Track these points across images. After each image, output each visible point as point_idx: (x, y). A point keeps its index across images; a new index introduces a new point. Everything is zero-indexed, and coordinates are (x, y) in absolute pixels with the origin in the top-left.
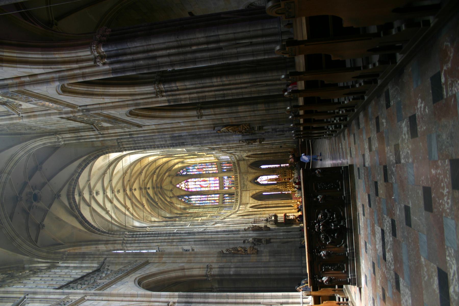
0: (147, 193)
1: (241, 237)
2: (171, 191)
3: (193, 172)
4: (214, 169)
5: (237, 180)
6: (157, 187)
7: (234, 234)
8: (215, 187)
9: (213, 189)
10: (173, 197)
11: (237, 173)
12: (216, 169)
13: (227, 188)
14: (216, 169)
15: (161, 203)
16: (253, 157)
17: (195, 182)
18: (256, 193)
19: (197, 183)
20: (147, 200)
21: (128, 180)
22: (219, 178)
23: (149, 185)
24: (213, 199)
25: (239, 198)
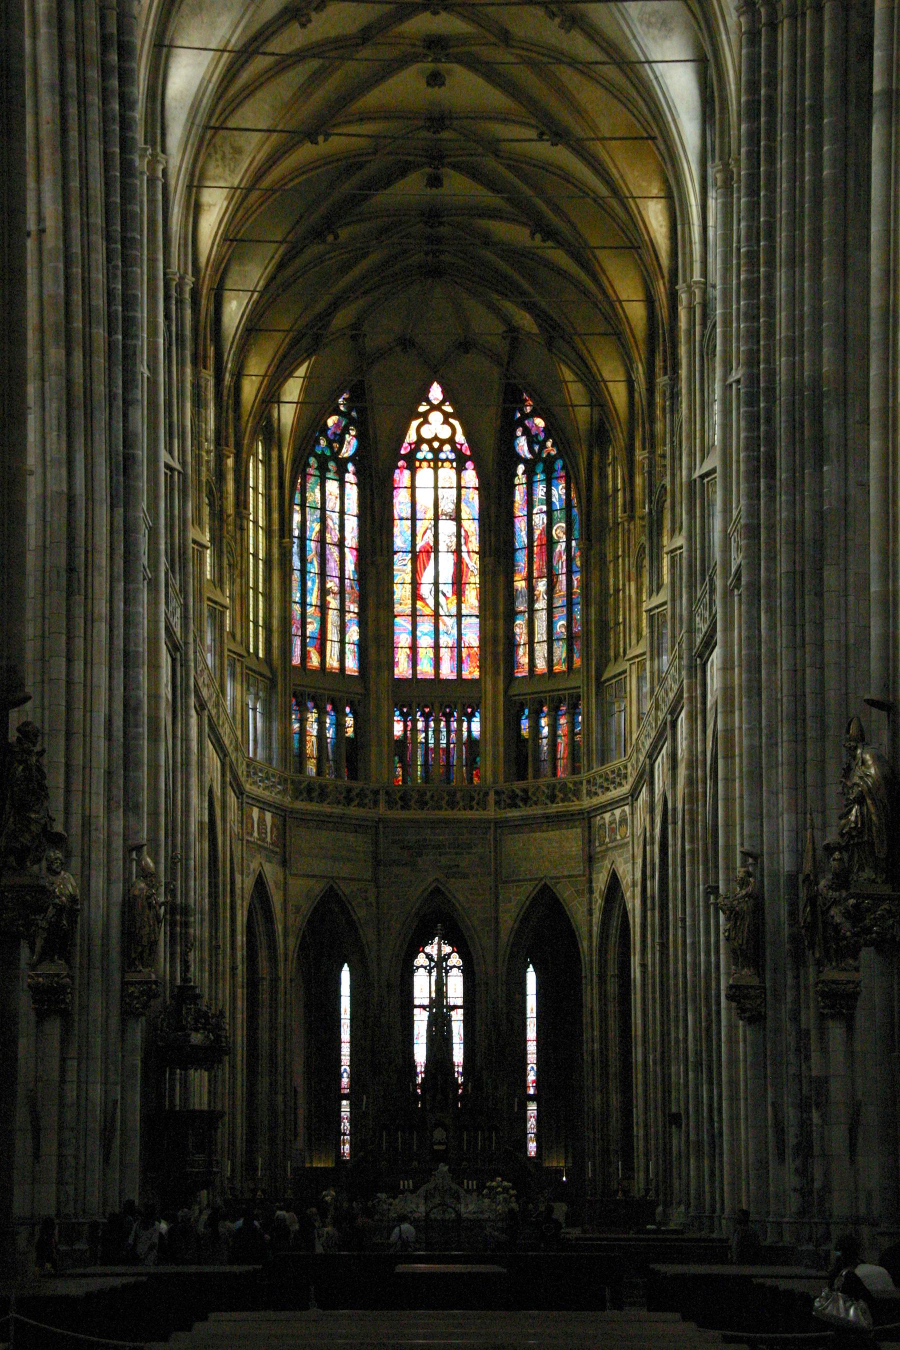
0: (404, 170)
1: (87, 823)
5: (452, 805)
7: (109, 773)
8: (414, 648)
9: (403, 639)
13: (398, 729)
17: (457, 518)
19: (447, 528)
21: (518, 30)
23: (458, 187)
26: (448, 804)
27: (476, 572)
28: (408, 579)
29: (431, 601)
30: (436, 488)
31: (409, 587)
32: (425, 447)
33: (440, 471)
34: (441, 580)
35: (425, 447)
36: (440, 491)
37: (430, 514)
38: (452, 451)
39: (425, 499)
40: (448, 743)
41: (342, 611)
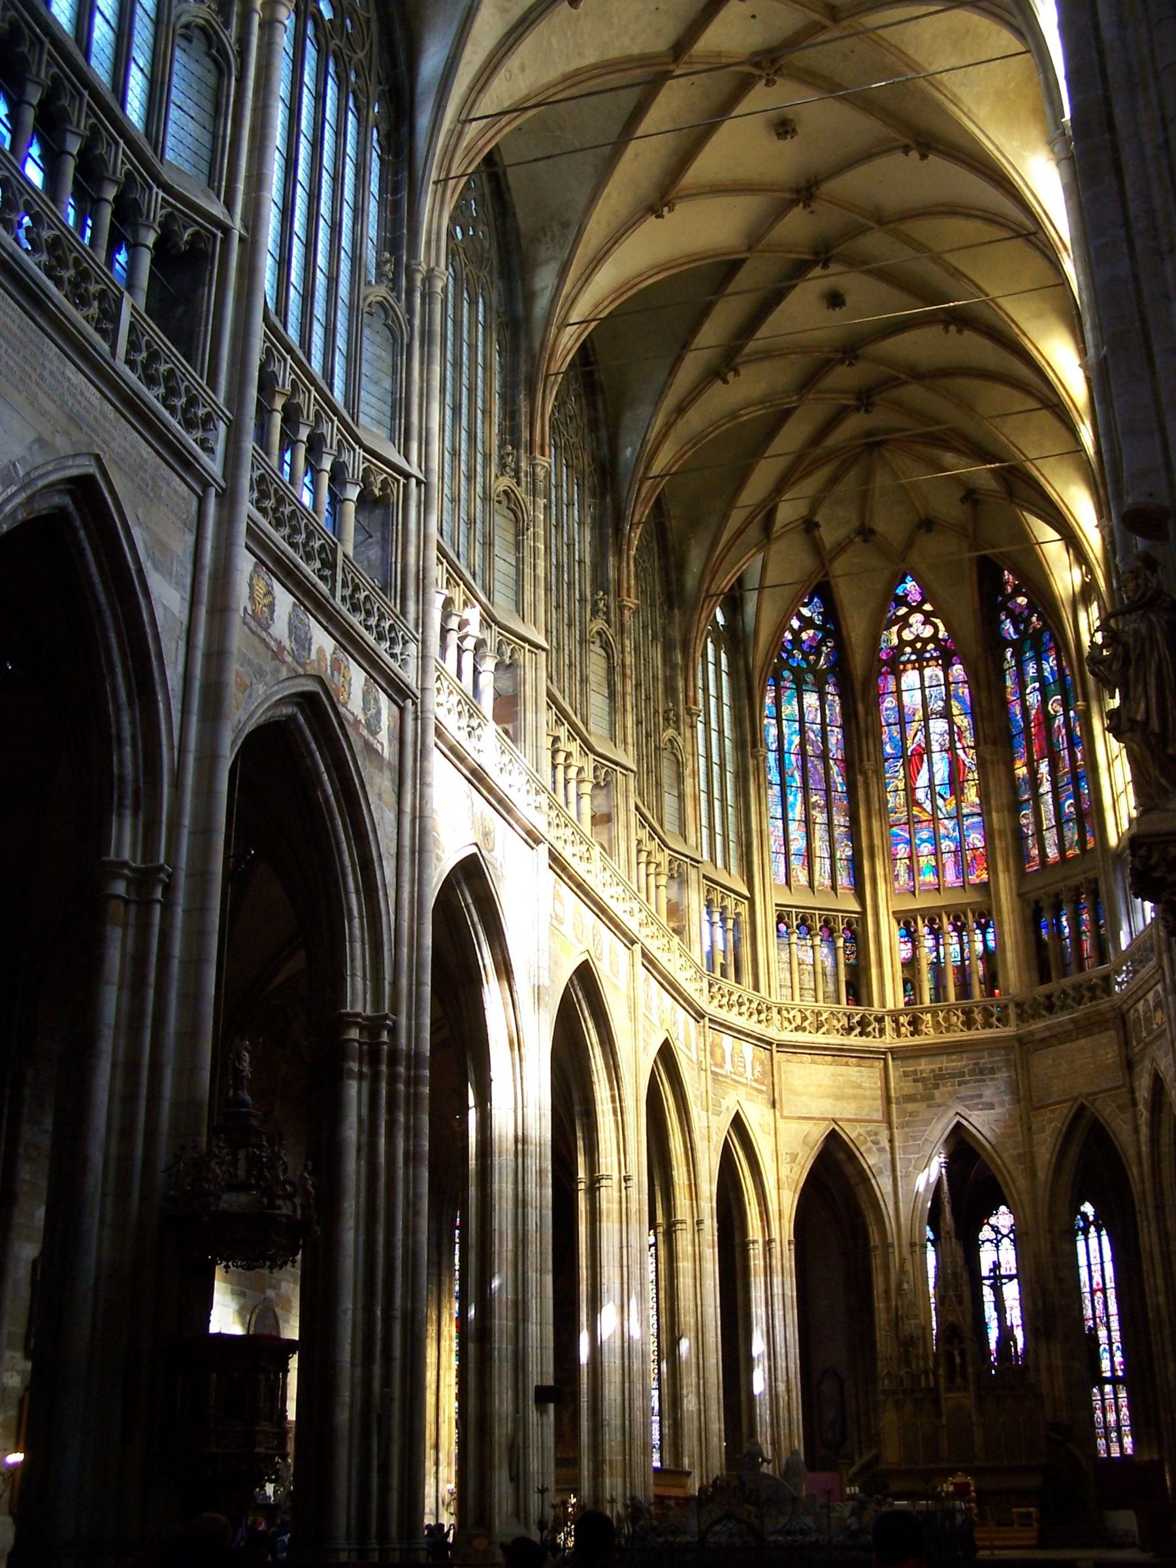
2: (866, 533)
3: (1022, 685)
4: (1051, 837)
5: (969, 1023)
6: (865, 399)
9: (902, 850)
10: (817, 548)
11: (1021, 1017)
12: (1052, 853)
14: (1052, 853)
15: (733, 415)
16: (1154, 1141)
17: (946, 714)
18: (863, 1177)
19: (938, 726)
20: (722, 271)
22: (984, 887)
24: (820, 847)
25: (819, 1039)
26: (963, 1023)
27: (974, 768)
28: (901, 785)
29: (928, 806)
30: (923, 688)
31: (902, 793)
32: (908, 650)
33: (928, 672)
34: (937, 782)
35: (908, 650)
36: (927, 690)
37: (919, 715)
38: (935, 650)
39: (912, 700)
40: (963, 960)
41: (830, 824)
